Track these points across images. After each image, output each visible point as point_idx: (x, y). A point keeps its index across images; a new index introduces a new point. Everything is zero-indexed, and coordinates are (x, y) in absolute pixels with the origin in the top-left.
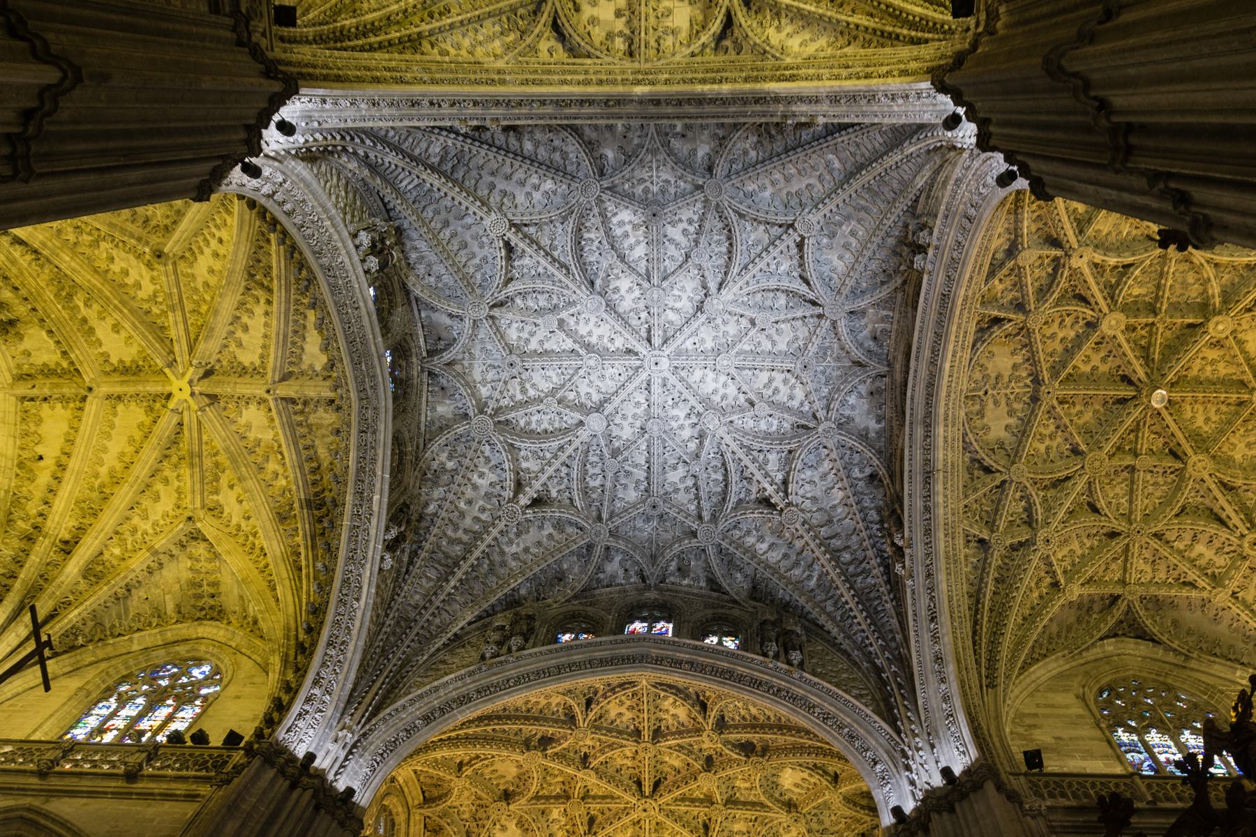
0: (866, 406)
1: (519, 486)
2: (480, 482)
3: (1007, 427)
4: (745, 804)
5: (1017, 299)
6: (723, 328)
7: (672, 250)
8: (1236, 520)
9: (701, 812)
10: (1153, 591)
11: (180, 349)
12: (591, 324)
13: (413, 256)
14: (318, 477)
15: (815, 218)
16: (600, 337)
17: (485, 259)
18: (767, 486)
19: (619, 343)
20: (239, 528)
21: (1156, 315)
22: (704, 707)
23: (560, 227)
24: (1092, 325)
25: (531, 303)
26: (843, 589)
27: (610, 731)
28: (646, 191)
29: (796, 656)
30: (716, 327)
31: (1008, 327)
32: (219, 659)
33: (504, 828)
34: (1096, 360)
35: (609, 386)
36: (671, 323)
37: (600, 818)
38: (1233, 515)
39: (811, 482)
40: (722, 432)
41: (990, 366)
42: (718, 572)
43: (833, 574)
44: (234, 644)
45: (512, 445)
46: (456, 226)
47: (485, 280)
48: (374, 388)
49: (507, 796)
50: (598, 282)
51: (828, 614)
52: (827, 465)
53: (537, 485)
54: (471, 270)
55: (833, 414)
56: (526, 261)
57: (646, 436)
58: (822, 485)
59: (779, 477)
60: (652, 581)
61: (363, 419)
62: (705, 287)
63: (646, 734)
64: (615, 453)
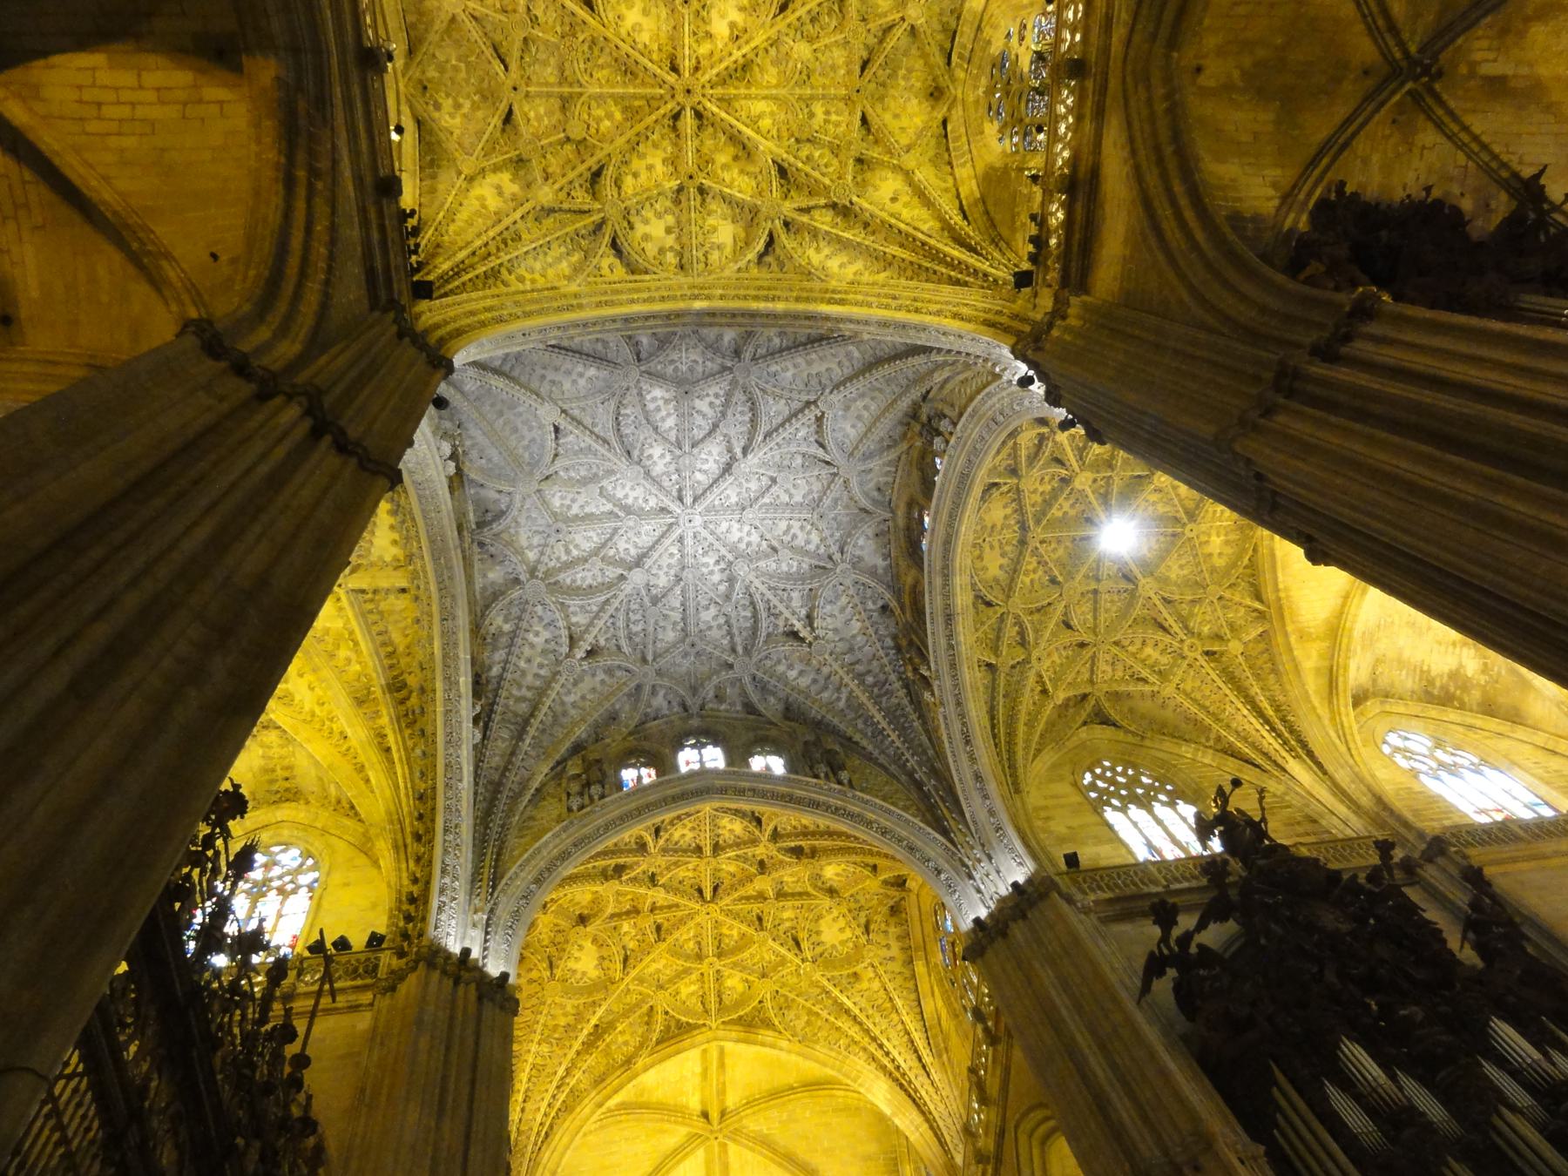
0: (873, 547)
2: (536, 640)
3: (1001, 567)
4: (793, 895)
5: (1010, 465)
7: (699, 420)
8: (1176, 628)
9: (756, 908)
10: (1115, 687)
12: (627, 488)
14: (395, 661)
15: (836, 398)
16: (636, 498)
17: (533, 440)
18: (795, 622)
19: (653, 502)
20: (313, 714)
21: (1113, 470)
24: (1065, 481)
26: (873, 710)
27: (676, 851)
28: (676, 370)
29: (844, 775)
31: (1005, 489)
32: (307, 842)
33: (581, 948)
34: (1066, 506)
35: (645, 541)
36: (698, 482)
37: (666, 925)
38: (1174, 624)
39: (832, 616)
40: (751, 577)
42: (755, 697)
43: (864, 698)
44: (319, 825)
49: (583, 920)
50: (636, 453)
51: (861, 732)
52: (844, 600)
53: (590, 638)
55: (848, 557)
56: (571, 438)
57: (682, 583)
58: (841, 618)
59: (803, 612)
60: (694, 710)
61: (443, 608)
62: (730, 450)
63: (708, 850)
64: (655, 601)
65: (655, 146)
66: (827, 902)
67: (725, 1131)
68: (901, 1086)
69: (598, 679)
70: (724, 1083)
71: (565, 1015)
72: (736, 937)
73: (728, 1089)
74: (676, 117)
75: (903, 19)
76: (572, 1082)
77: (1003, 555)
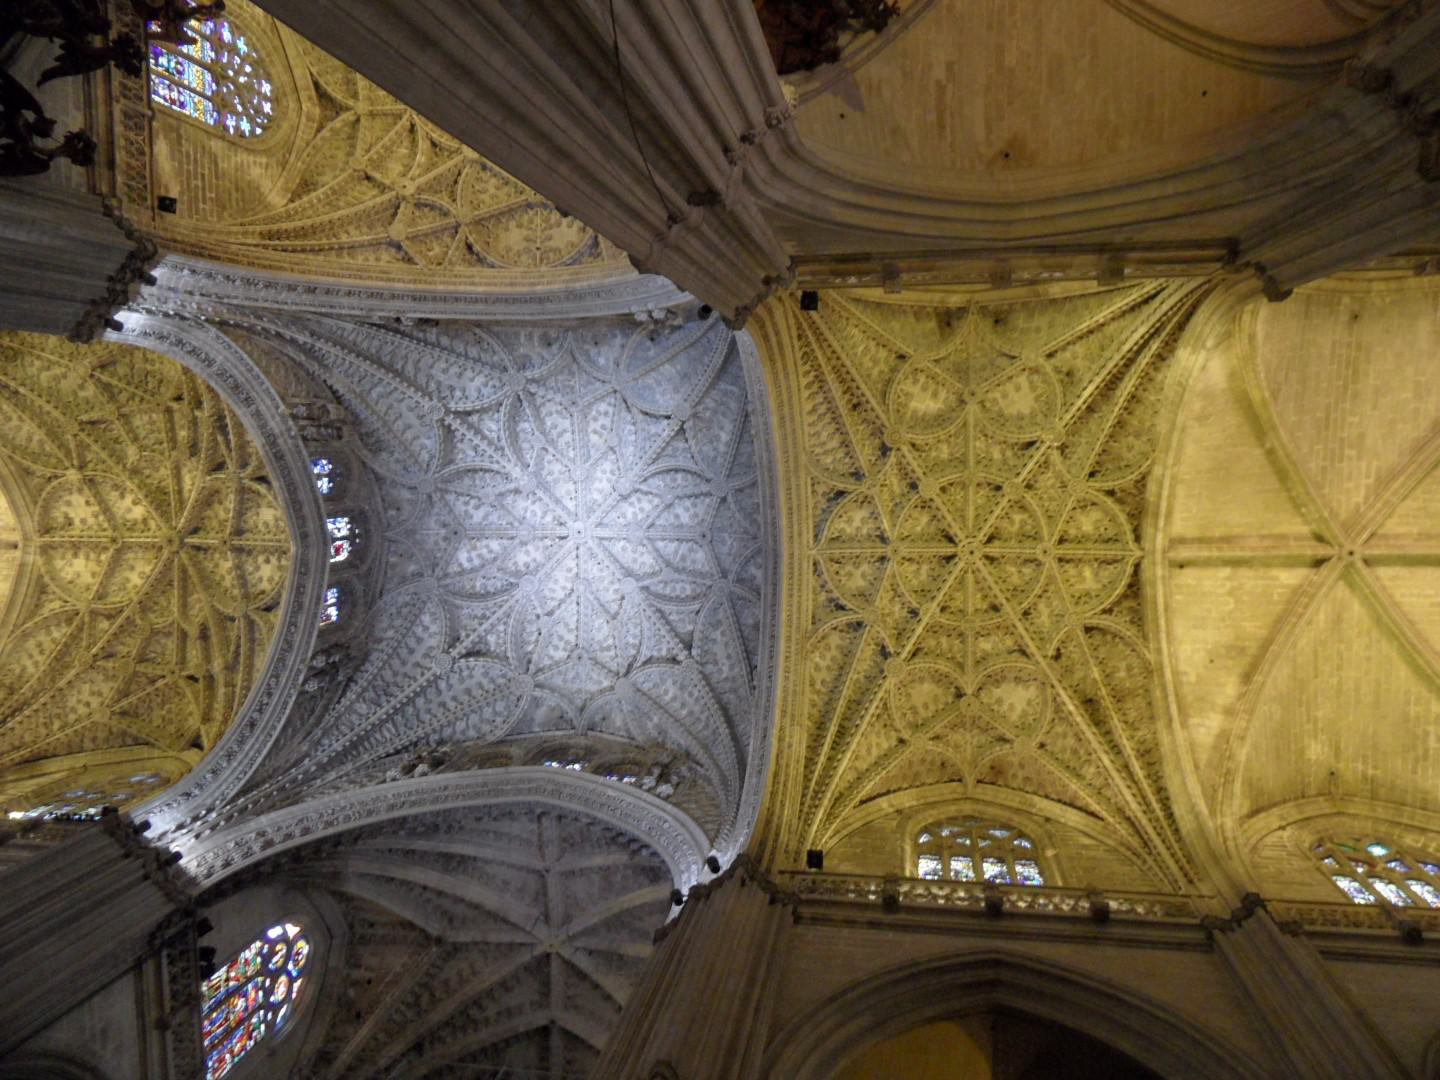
1: (674, 660)
2: (670, 694)
3: (570, 226)
6: (556, 475)
7: (493, 518)
11: (519, 938)
13: (472, 733)
16: (567, 579)
19: (570, 563)
22: (841, 494)
23: (465, 611)
25: (533, 638)
30: (556, 481)
31: (471, 240)
41: (516, 248)
45: (645, 663)
46: (447, 696)
47: (504, 676)
48: (530, 781)
49: (959, 695)
54: (492, 686)
56: (492, 639)
65: (217, 566)
66: (972, 408)
67: (1341, 539)
68: (1181, 327)
69: (719, 638)
70: (1263, 537)
71: (1065, 736)
72: (1025, 516)
73: (1277, 530)
74: (198, 548)
75: (92, 376)
76: (1128, 748)
77: (559, 225)
